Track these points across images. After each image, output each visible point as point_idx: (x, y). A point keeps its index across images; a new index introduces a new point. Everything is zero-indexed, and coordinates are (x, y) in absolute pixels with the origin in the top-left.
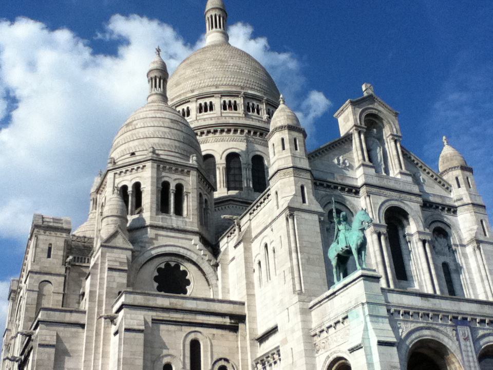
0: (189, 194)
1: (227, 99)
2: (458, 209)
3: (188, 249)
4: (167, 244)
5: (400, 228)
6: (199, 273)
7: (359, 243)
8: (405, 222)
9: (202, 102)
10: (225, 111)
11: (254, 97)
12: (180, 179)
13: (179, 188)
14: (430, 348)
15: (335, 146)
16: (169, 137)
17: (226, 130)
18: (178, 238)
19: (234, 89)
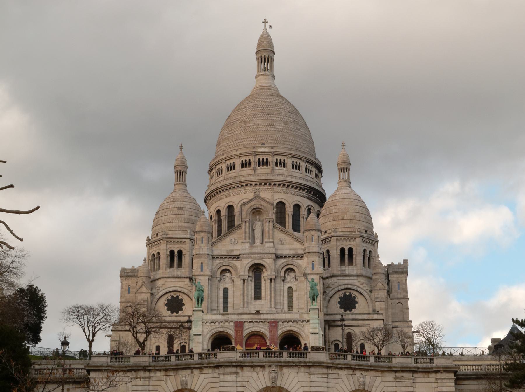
0: (185, 255)
2: (304, 255)
3: (182, 287)
4: (171, 286)
5: (262, 273)
6: (189, 299)
7: (197, 296)
8: (264, 270)
9: (228, 162)
11: (263, 153)
12: (180, 247)
13: (180, 252)
14: (223, 334)
16: (175, 221)
17: (240, 186)
19: (248, 151)
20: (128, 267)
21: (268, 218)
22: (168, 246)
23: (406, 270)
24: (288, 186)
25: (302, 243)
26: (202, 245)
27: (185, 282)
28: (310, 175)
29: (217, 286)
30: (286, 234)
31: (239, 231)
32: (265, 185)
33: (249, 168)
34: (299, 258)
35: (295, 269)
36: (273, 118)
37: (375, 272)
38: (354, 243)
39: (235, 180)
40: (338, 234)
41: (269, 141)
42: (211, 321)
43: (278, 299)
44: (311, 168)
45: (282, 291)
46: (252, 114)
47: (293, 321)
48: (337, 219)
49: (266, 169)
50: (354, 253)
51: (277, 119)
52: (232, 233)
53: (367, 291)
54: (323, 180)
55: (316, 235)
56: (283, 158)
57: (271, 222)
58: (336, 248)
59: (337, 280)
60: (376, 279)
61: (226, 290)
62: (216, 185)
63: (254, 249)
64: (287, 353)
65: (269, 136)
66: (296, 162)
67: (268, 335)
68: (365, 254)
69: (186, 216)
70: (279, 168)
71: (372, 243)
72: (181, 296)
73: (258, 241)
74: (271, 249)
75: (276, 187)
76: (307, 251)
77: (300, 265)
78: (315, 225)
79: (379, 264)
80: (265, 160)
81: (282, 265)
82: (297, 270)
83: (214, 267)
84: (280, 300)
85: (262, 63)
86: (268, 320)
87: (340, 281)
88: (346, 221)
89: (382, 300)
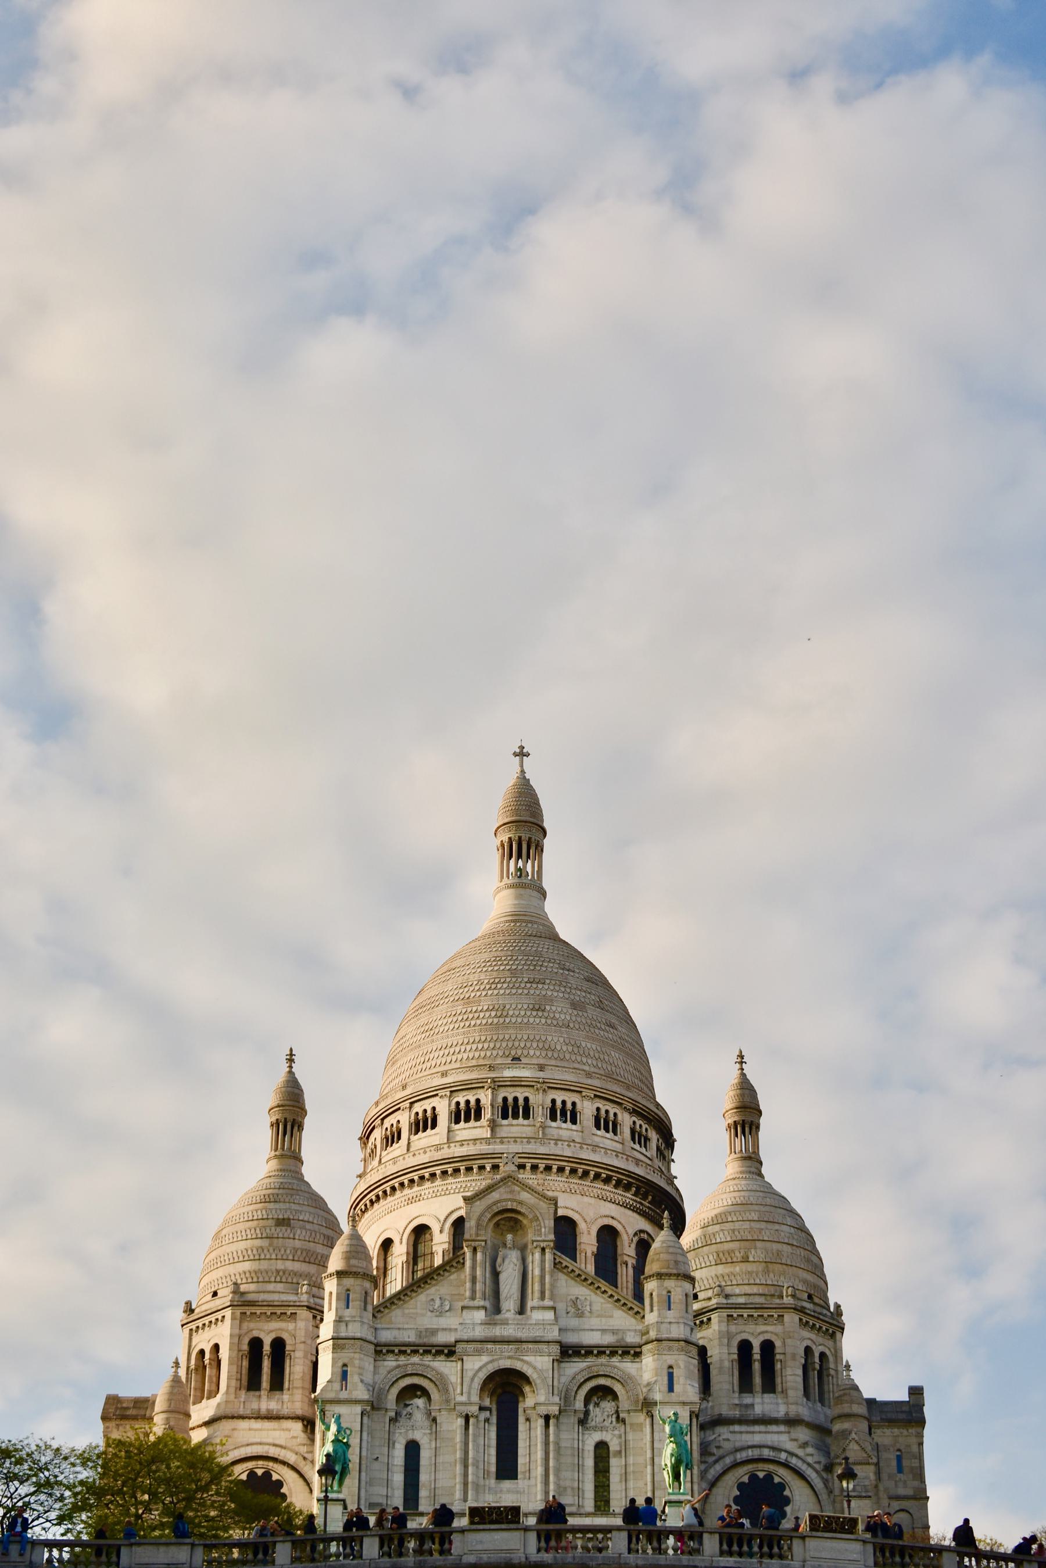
0: (292, 1353)
1: (461, 1098)
2: (645, 1348)
5: (521, 1399)
6: (301, 1481)
8: (527, 1389)
9: (418, 1108)
10: (457, 1127)
11: (516, 1083)
12: (280, 1329)
13: (279, 1345)
15: (429, 1282)
16: (268, 1257)
17: (450, 1171)
18: (268, 1430)
19: (474, 1075)
20: (129, 1391)
21: (539, 1239)
22: (245, 1325)
23: (919, 1415)
24: (586, 1173)
25: (639, 1315)
26: (347, 1313)
27: (289, 1430)
28: (643, 1150)
29: (387, 1436)
30: (591, 1287)
31: (452, 1277)
32: (521, 1171)
33: (478, 1124)
34: (629, 1358)
35: (617, 1388)
36: (544, 993)
37: (837, 1410)
38: (778, 1329)
39: (438, 1155)
40: (729, 1301)
41: (532, 1052)
43: (569, 1477)
44: (646, 1130)
45: (579, 1453)
46: (486, 981)
48: (729, 1260)
49: (523, 1125)
50: (778, 1357)
51: (555, 994)
52: (434, 1282)
53: (817, 1466)
54: (675, 1169)
55: (679, 1290)
56: (570, 1098)
58: (726, 1341)
59: (731, 1432)
60: (845, 1434)
61: (413, 1449)
62: (384, 1170)
63: (498, 1327)
64: (717, 1536)
65: (531, 1037)
66: (607, 1112)
68: (809, 1361)
69: (298, 1244)
70: (559, 1123)
71: (827, 1330)
72: (279, 1473)
73: (509, 1304)
75: (553, 1177)
77: (630, 1377)
78: (676, 1262)
79: (849, 1389)
80: (521, 1102)
82: (624, 1392)
83: (378, 1378)
84: (573, 1480)
85: (511, 857)
87: (738, 1436)
88: (754, 1264)
89: (864, 1494)
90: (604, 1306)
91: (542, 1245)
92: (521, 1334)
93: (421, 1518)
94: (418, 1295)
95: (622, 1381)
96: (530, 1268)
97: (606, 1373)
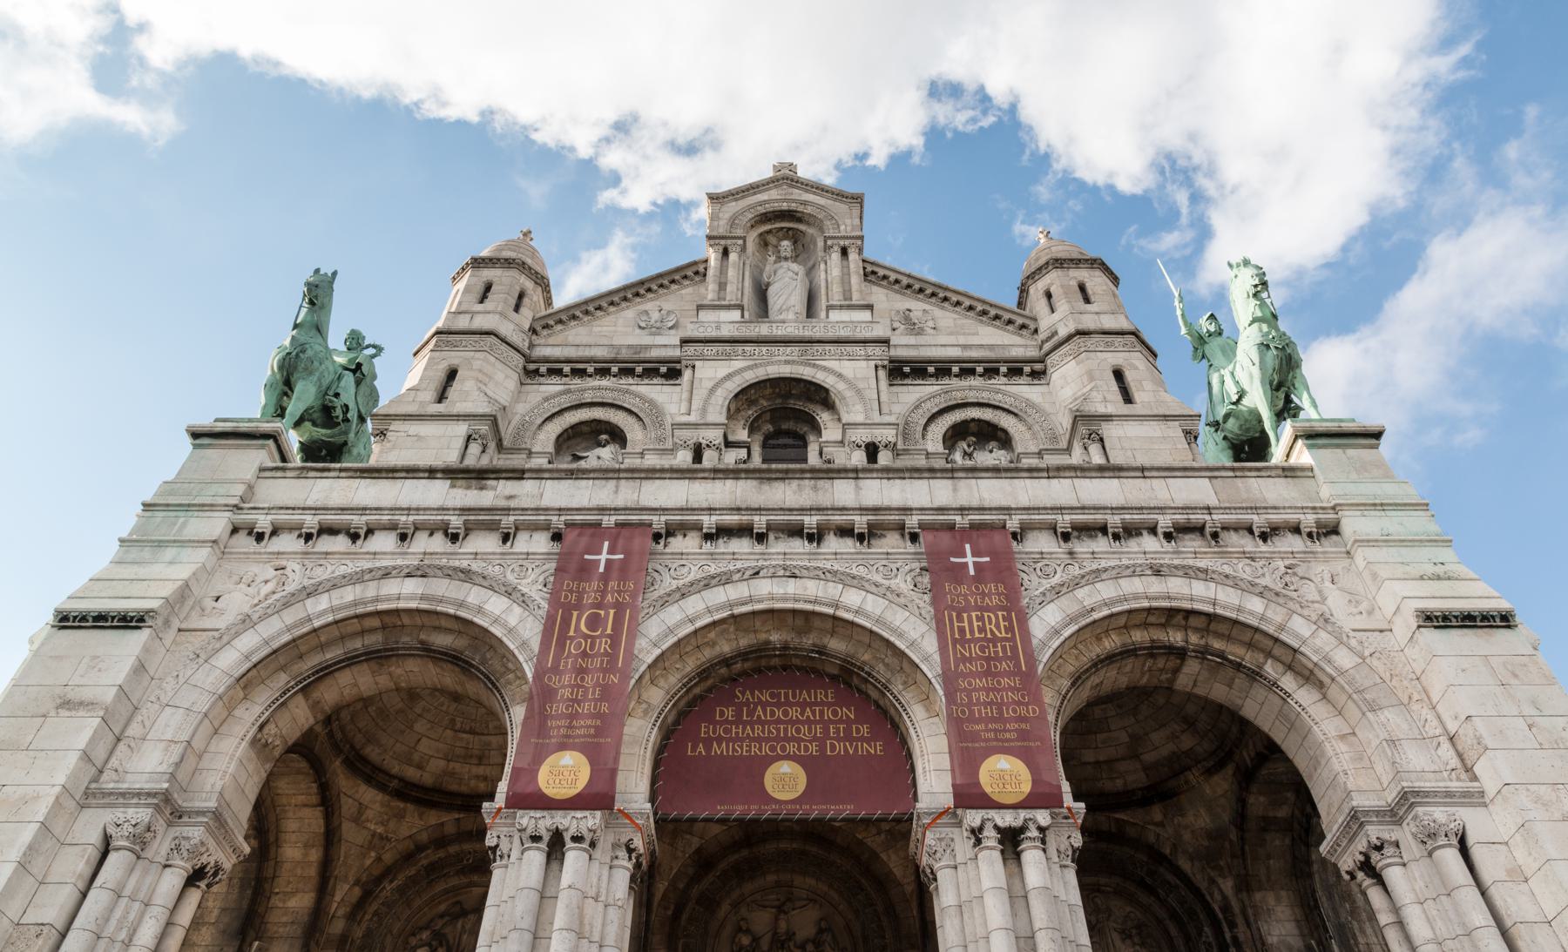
2: (1048, 362)
5: (811, 438)
8: (824, 417)
26: (480, 307)
30: (933, 300)
31: (683, 292)
34: (1017, 380)
35: (1006, 422)
42: (330, 518)
47: (1165, 522)
52: (650, 295)
57: (849, 250)
67: (930, 645)
74: (863, 325)
76: (1063, 332)
81: (928, 404)
82: (1021, 427)
83: (521, 408)
86: (906, 510)
90: (959, 322)
91: (842, 243)
92: (811, 333)
93: (509, 483)
94: (623, 309)
95: (1016, 411)
96: (823, 275)
97: (981, 401)
